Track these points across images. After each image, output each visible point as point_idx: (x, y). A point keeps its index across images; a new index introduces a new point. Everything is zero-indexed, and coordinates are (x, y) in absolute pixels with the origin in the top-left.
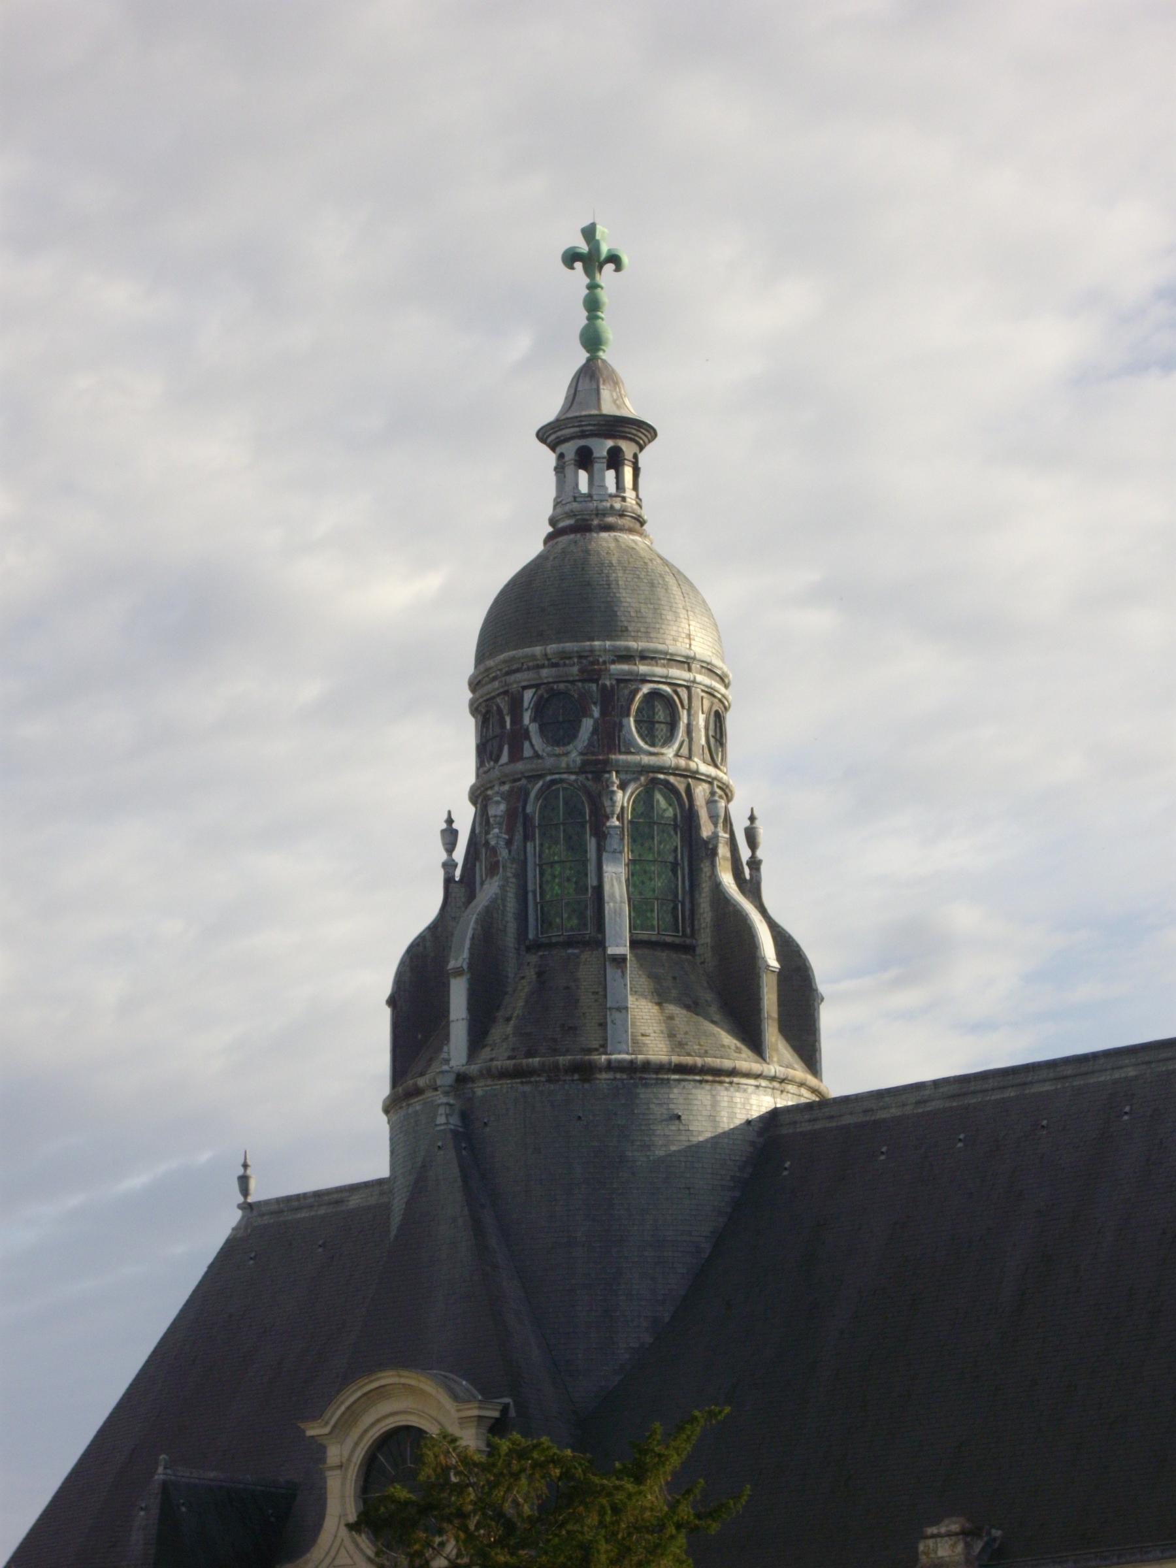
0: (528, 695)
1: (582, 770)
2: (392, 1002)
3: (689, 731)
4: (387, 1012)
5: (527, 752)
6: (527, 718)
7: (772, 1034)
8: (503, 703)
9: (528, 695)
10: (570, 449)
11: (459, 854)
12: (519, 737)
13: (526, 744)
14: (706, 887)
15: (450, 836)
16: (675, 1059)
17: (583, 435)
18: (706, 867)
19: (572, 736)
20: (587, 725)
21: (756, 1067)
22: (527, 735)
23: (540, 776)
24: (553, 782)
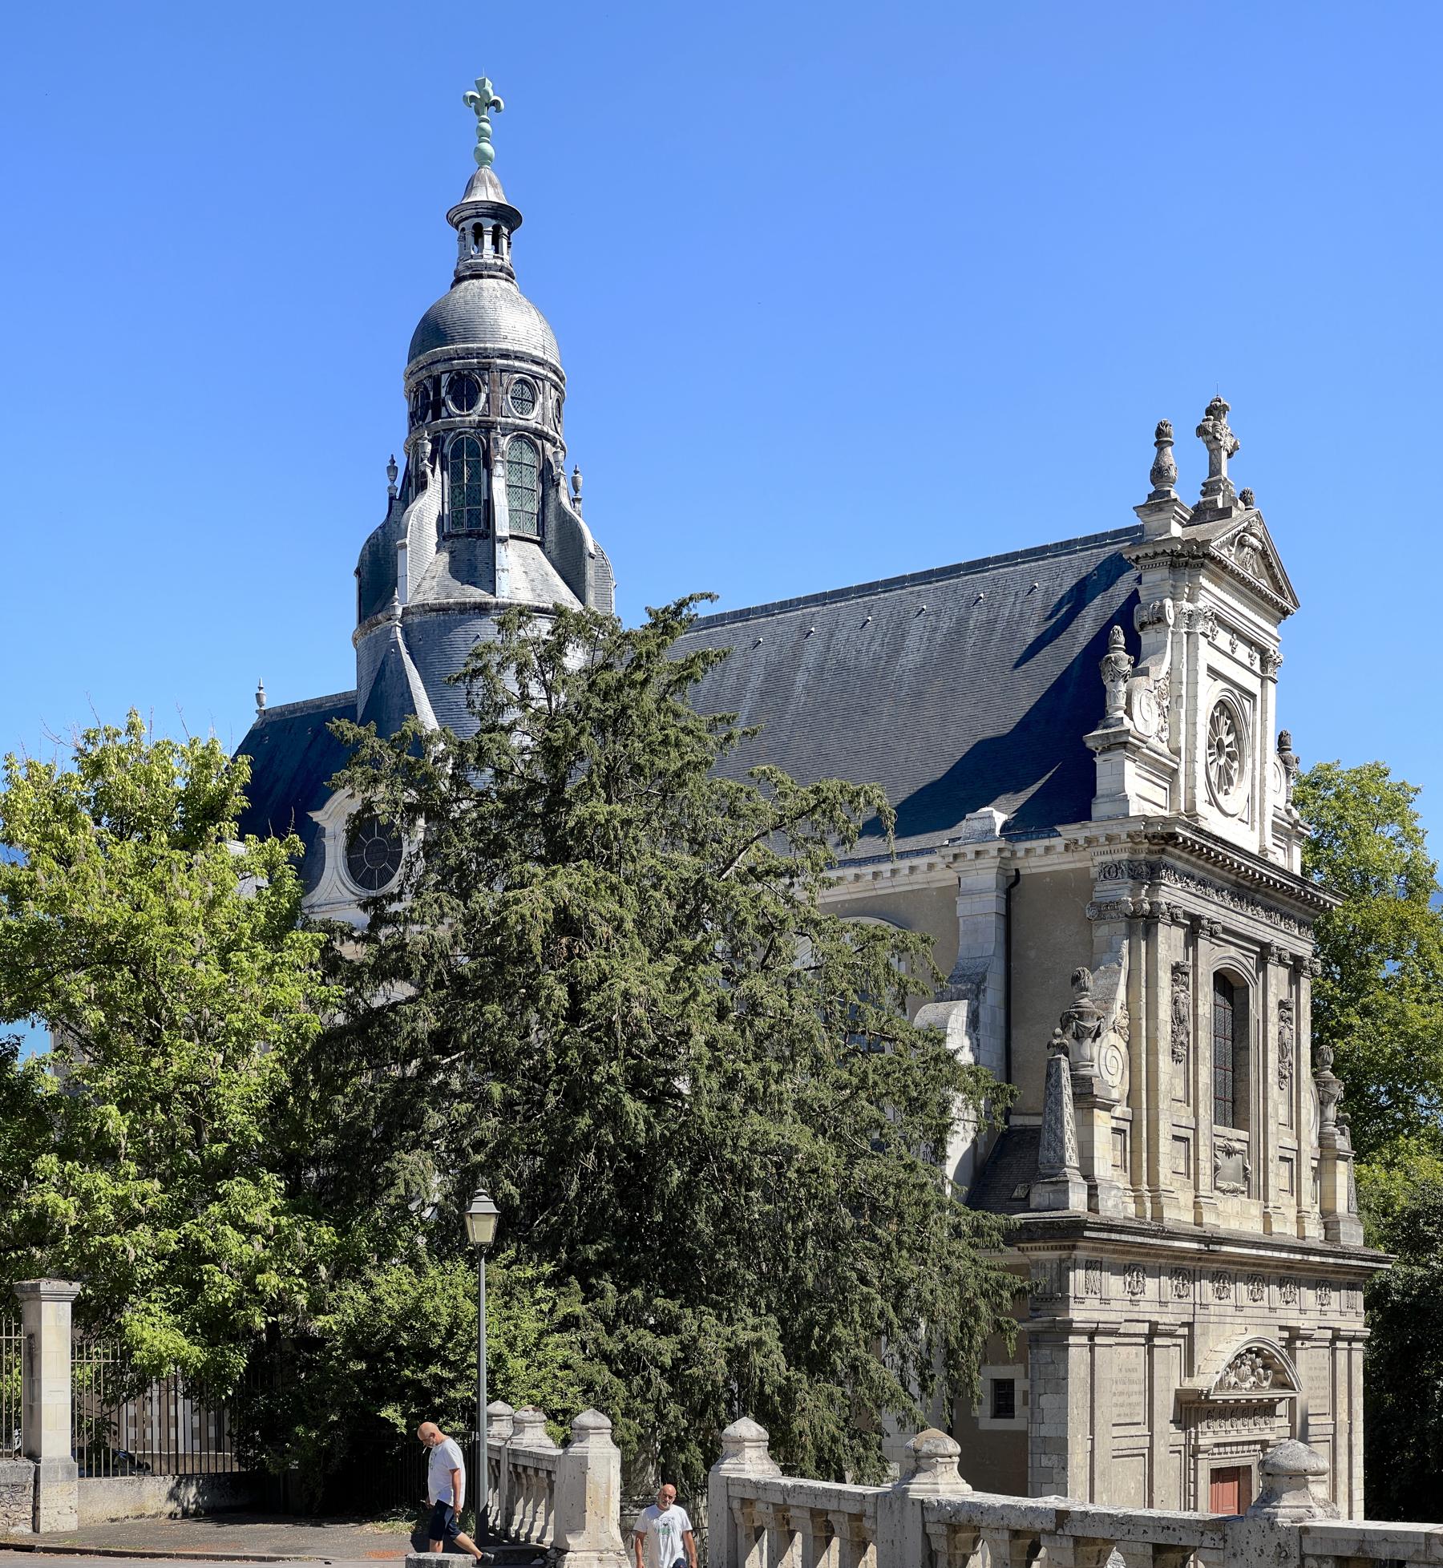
0: (445, 378)
1: (479, 427)
5: (444, 413)
6: (443, 394)
8: (428, 383)
9: (445, 378)
12: (437, 406)
20: (483, 397)
22: (444, 404)
23: (451, 430)
24: (461, 433)
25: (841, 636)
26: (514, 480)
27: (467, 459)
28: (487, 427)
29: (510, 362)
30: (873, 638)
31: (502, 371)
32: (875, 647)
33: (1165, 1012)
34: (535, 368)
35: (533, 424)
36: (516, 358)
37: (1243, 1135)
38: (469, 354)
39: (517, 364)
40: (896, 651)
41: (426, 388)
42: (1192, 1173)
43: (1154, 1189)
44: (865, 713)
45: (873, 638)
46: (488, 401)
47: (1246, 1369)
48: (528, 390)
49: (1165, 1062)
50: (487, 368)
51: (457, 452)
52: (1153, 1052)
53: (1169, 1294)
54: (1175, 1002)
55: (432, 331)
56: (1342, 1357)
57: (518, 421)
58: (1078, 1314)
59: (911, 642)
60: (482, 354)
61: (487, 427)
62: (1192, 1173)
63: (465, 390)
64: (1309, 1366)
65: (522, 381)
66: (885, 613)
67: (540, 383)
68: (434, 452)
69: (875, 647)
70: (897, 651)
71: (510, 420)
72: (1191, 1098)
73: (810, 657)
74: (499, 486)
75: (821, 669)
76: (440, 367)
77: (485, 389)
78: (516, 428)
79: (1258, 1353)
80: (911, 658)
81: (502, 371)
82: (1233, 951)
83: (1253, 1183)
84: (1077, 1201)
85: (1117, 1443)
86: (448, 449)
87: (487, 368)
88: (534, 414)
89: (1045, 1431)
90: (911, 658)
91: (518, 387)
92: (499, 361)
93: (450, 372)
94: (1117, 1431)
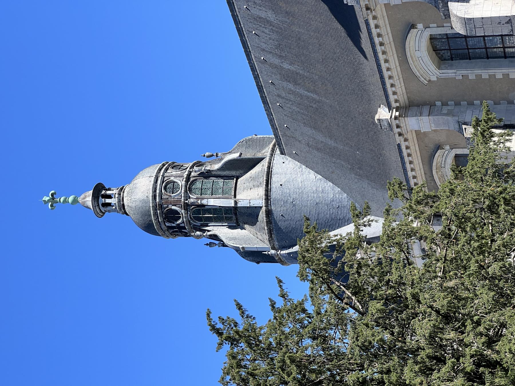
0: (167, 224)
2: (258, 263)
3: (176, 177)
4: (262, 264)
5: (182, 225)
6: (175, 225)
7: (259, 155)
9: (167, 224)
10: (103, 209)
11: (217, 242)
13: (181, 225)
14: (219, 173)
15: (210, 245)
16: (264, 186)
17: (99, 205)
18: (213, 173)
19: (177, 212)
21: (267, 160)
22: (179, 225)
23: (189, 222)
24: (191, 218)
25: (264, 46)
26: (209, 192)
27: (202, 216)
28: (186, 206)
29: (157, 195)
30: (263, 32)
31: (161, 199)
32: (267, 31)
34: (159, 182)
35: (184, 183)
36: (155, 191)
38: (155, 214)
39: (158, 191)
40: (268, 22)
41: (173, 232)
44: (299, 39)
45: (263, 32)
46: (175, 205)
48: (169, 186)
50: (161, 206)
51: (200, 219)
55: (149, 228)
57: (183, 191)
59: (263, 15)
60: (155, 208)
61: (186, 206)
63: (172, 216)
65: (165, 188)
66: (250, 25)
67: (166, 178)
68: (201, 230)
69: (267, 31)
70: (268, 21)
71: (183, 195)
73: (276, 61)
74: (212, 202)
75: (280, 57)
76: (163, 226)
77: (170, 206)
78: (186, 191)
80: (270, 16)
81: (161, 199)
86: (198, 223)
87: (161, 206)
88: (179, 182)
90: (270, 16)
91: (168, 190)
92: (157, 200)
93: (164, 222)
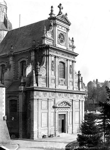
33: (50, 66)
37: (65, 79)
42: (55, 82)
43: (49, 85)
47: (64, 104)
49: (50, 71)
52: (48, 70)
53: (51, 95)
54: (52, 65)
56: (81, 103)
58: (35, 97)
62: (55, 82)
64: (76, 104)
72: (55, 75)
79: (65, 102)
82: (62, 60)
83: (66, 84)
84: (35, 85)
85: (42, 111)
89: (32, 110)
94: (42, 110)
